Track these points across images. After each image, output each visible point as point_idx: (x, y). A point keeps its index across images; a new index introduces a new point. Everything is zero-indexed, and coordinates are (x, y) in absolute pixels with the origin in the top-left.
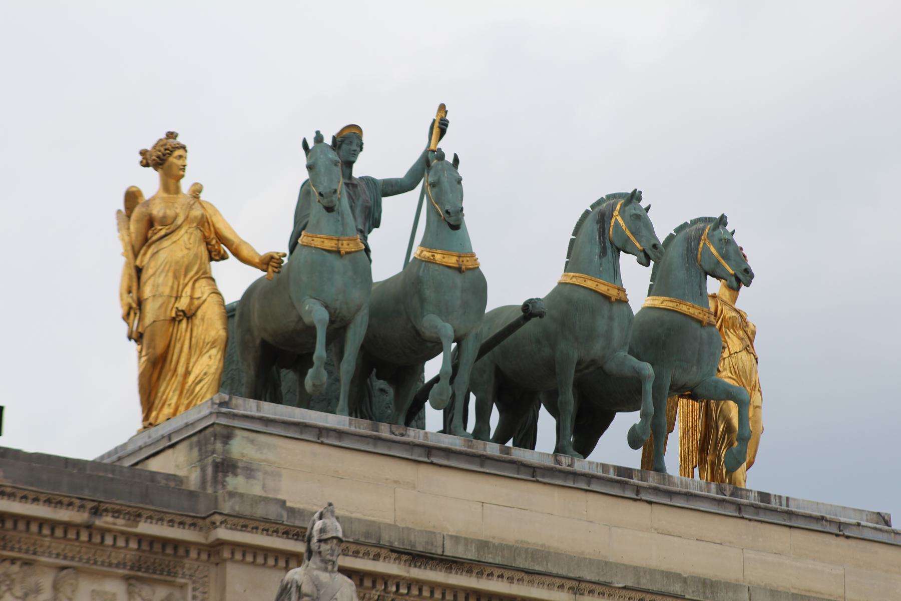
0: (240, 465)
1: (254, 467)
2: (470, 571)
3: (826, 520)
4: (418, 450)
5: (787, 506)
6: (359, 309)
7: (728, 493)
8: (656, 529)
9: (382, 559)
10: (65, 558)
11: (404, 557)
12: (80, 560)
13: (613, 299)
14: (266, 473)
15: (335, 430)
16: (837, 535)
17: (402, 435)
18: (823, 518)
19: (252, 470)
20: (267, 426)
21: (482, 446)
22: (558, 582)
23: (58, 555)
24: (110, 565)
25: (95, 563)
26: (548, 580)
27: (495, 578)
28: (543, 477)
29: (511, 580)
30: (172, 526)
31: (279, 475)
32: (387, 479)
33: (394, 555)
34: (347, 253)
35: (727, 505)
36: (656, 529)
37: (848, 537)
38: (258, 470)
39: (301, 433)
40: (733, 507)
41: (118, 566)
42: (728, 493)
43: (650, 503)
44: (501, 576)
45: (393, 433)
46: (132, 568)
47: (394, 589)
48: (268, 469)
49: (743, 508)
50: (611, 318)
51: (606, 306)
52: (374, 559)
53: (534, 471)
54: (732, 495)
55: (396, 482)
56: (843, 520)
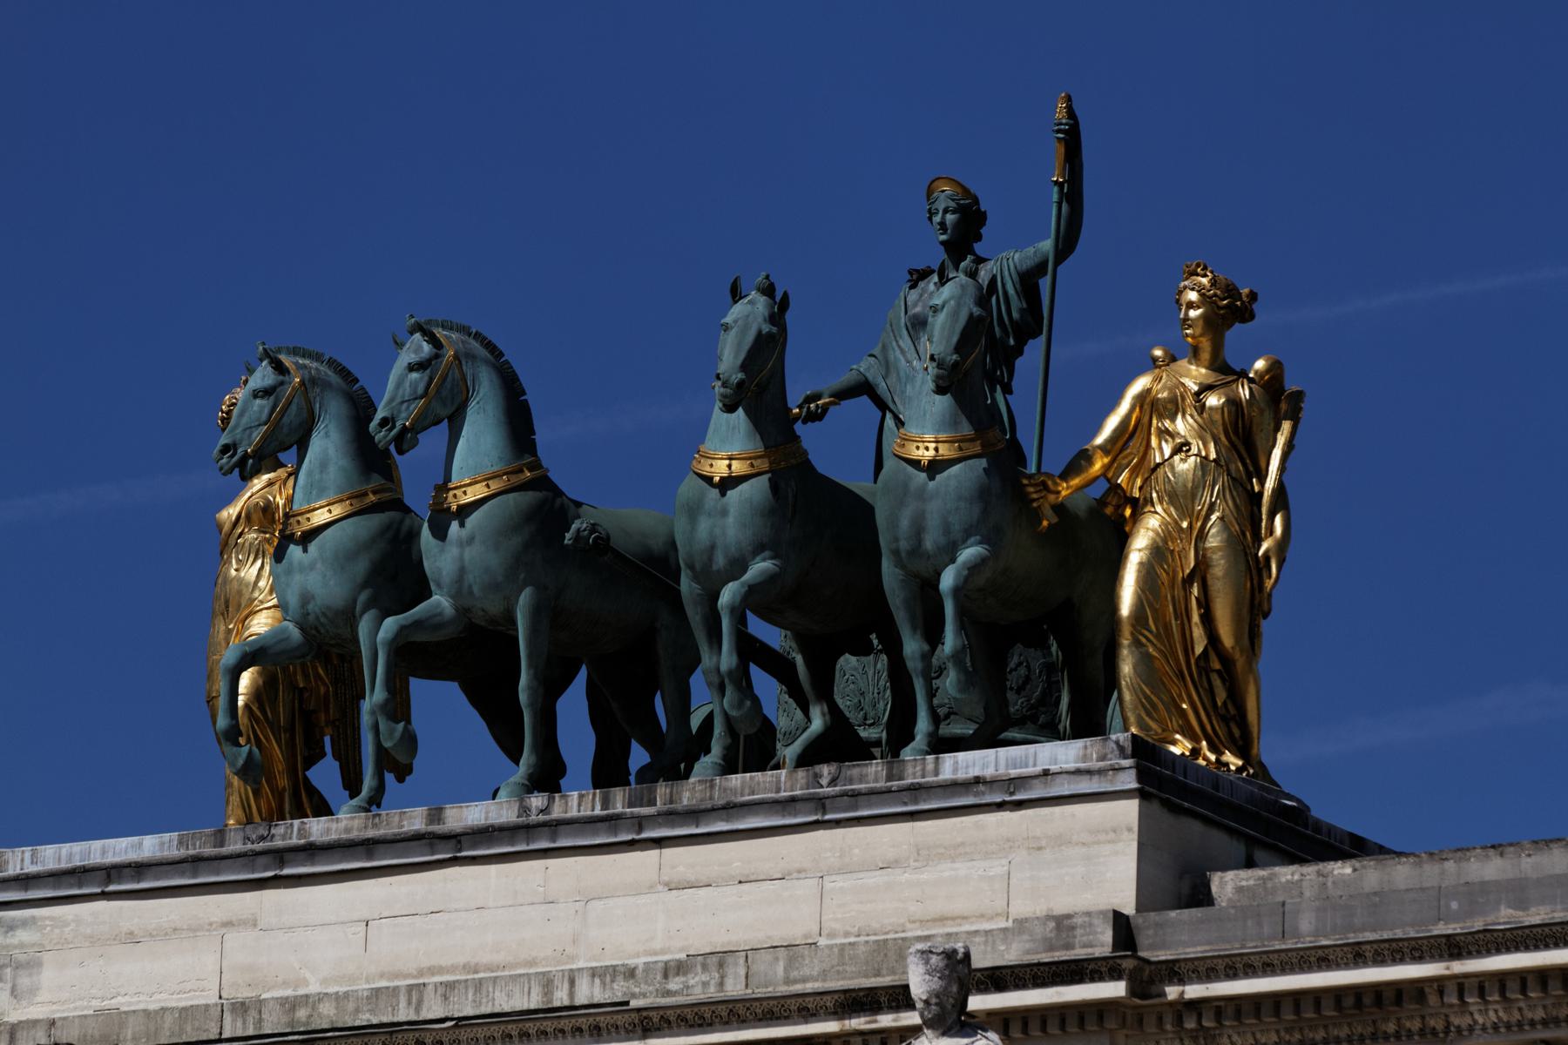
4: (262, 860)
5: (936, 773)
8: (666, 884)
14: (18, 966)
15: (129, 865)
16: (1000, 806)
17: (262, 838)
18: (978, 780)
20: (26, 890)
28: (474, 847)
31: (39, 964)
35: (799, 805)
36: (666, 884)
37: (1020, 805)
40: (811, 805)
42: (824, 782)
43: (659, 843)
45: (247, 839)
48: (22, 958)
49: (827, 802)
50: (724, 513)
51: (715, 492)
55: (228, 924)
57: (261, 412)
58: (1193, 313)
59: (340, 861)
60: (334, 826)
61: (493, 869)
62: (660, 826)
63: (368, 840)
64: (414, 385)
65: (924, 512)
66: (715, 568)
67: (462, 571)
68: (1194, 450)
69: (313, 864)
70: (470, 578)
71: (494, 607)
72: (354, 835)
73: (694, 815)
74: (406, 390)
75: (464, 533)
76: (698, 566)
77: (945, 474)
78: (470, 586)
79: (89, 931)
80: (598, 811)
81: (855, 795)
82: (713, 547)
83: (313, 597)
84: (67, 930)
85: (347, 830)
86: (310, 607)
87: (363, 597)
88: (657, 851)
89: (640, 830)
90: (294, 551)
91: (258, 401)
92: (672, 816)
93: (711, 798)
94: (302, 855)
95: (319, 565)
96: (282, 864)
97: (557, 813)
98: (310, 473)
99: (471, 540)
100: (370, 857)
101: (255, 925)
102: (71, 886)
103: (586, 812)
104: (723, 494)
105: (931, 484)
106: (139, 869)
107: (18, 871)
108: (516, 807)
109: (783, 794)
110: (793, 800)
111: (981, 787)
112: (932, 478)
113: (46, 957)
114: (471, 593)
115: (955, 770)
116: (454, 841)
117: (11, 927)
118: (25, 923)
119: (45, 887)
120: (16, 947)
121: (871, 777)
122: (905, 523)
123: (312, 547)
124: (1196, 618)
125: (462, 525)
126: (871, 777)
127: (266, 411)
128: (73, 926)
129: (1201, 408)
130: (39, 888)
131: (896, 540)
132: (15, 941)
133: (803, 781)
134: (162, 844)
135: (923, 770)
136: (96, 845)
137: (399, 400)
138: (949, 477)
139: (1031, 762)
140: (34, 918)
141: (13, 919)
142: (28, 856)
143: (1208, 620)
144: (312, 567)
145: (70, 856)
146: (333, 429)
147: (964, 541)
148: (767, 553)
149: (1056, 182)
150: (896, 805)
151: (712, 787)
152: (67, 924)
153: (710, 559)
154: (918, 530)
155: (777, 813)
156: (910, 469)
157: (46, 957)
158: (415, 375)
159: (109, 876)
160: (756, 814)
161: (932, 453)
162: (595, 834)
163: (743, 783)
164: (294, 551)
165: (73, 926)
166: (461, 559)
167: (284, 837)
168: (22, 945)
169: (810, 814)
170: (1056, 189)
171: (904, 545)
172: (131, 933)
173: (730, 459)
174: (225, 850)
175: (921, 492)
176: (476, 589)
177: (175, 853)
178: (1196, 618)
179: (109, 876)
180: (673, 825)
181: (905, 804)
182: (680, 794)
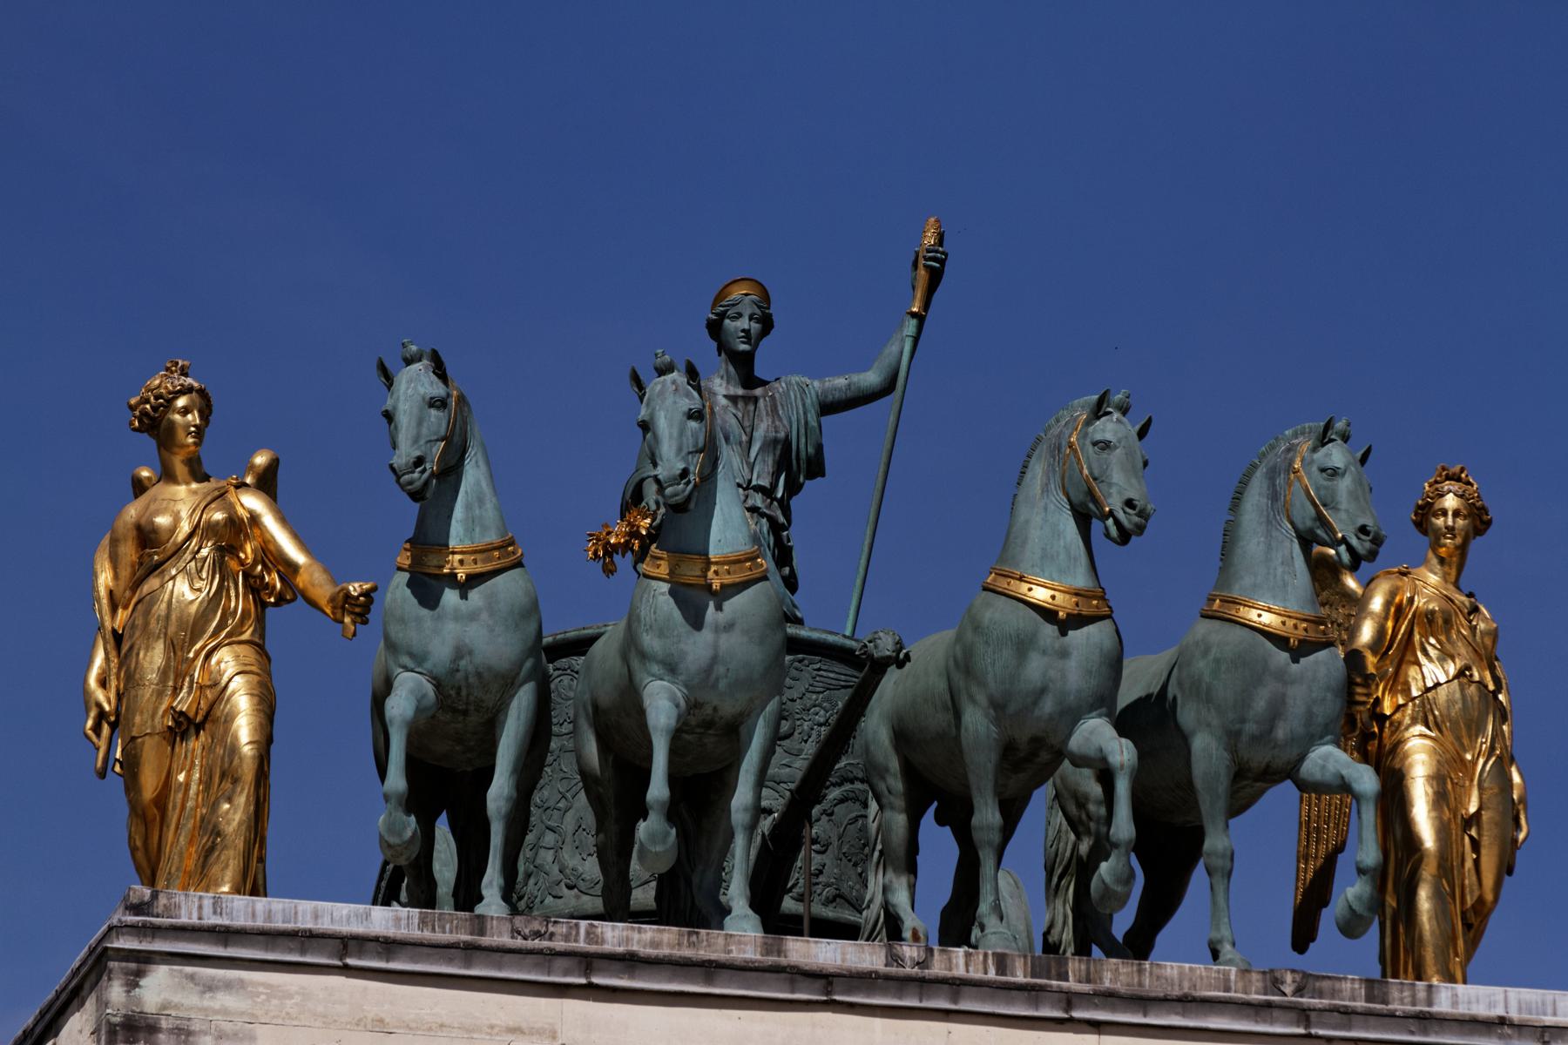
0: (164, 1024)
1: (195, 1027)
3: (1512, 1025)
4: (560, 963)
5: (1430, 1004)
6: (509, 684)
7: (1288, 989)
13: (1061, 614)
15: (376, 939)
17: (537, 935)
18: (1502, 1021)
19: (189, 1033)
20: (226, 946)
21: (721, 941)
28: (848, 992)
32: (492, 1027)
34: (475, 580)
35: (1276, 1013)
38: (205, 1033)
39: (303, 952)
40: (1293, 1015)
42: (1288, 989)
43: (1097, 1027)
45: (515, 932)
48: (227, 1027)
49: (1313, 1015)
50: (1064, 654)
51: (1050, 630)
53: (831, 983)
54: (1299, 991)
55: (515, 1030)
56: (1549, 1020)
57: (440, 425)
58: (1460, 522)
59: (670, 981)
60: (636, 936)
61: (878, 1023)
62: (1096, 1007)
63: (710, 962)
64: (695, 435)
65: (1284, 695)
66: (1037, 712)
67: (715, 660)
68: (1476, 677)
69: (632, 977)
70: (720, 669)
71: (728, 708)
72: (665, 951)
73: (1141, 1001)
74: (689, 444)
75: (722, 617)
76: (1012, 708)
77: (1312, 658)
78: (717, 679)
79: (320, 1009)
80: (992, 974)
81: (1347, 1012)
82: (1042, 691)
83: (471, 653)
84: (289, 1002)
85: (655, 944)
86: (463, 663)
87: (529, 664)
88: (1095, 1037)
89: (1069, 1006)
90: (450, 597)
91: (433, 412)
92: (1110, 998)
93: (1140, 984)
94: (617, 965)
95: (484, 616)
96: (588, 970)
97: (937, 969)
98: (468, 507)
99: (729, 627)
100: (709, 980)
101: (554, 1037)
102: (291, 951)
103: (976, 974)
104: (1064, 633)
105: (1294, 666)
106: (389, 946)
107: (195, 920)
108: (883, 954)
109: (1232, 994)
110: (1269, 1005)
111: (1507, 1030)
112: (1295, 660)
113: (260, 1030)
114: (714, 686)
115: (1455, 1003)
116: (820, 983)
117: (210, 987)
118: (228, 986)
119: (252, 946)
120: (217, 1012)
121: (1347, 994)
122: (1260, 704)
123: (474, 595)
124: (1469, 864)
125: (719, 608)
126: (1347, 994)
127: (444, 425)
128: (297, 999)
129: (1473, 629)
130: (244, 946)
131: (1243, 721)
132: (216, 1005)
133: (1260, 985)
134: (398, 920)
135: (1413, 996)
136: (1515, 994)
137: (685, 451)
138: (1316, 662)
139: (1550, 1010)
140: (241, 982)
141: (213, 979)
142: (208, 903)
143: (1477, 862)
144: (472, 617)
145: (269, 915)
146: (480, 455)
147: (1321, 737)
148: (1104, 710)
149: (913, 315)
150: (1400, 1032)
151: (1140, 971)
152: (290, 996)
153: (1035, 703)
154: (1276, 711)
155: (1247, 1017)
156: (1269, 645)
157: (260, 1030)
158: (693, 424)
159: (345, 947)
160: (1221, 1014)
161: (1301, 633)
162: (1010, 1002)
163: (1181, 974)
164: (450, 597)
165: (297, 999)
166: (716, 647)
167: (567, 938)
168: (225, 1011)
169: (1290, 1024)
170: (914, 322)
171: (1251, 728)
172: (381, 1021)
173: (1077, 594)
174: (486, 941)
175: (1281, 676)
176: (722, 685)
177: (415, 933)
178: (1469, 864)
179: (345, 947)
180: (1114, 1009)
181: (1412, 1033)
182: (1099, 973)
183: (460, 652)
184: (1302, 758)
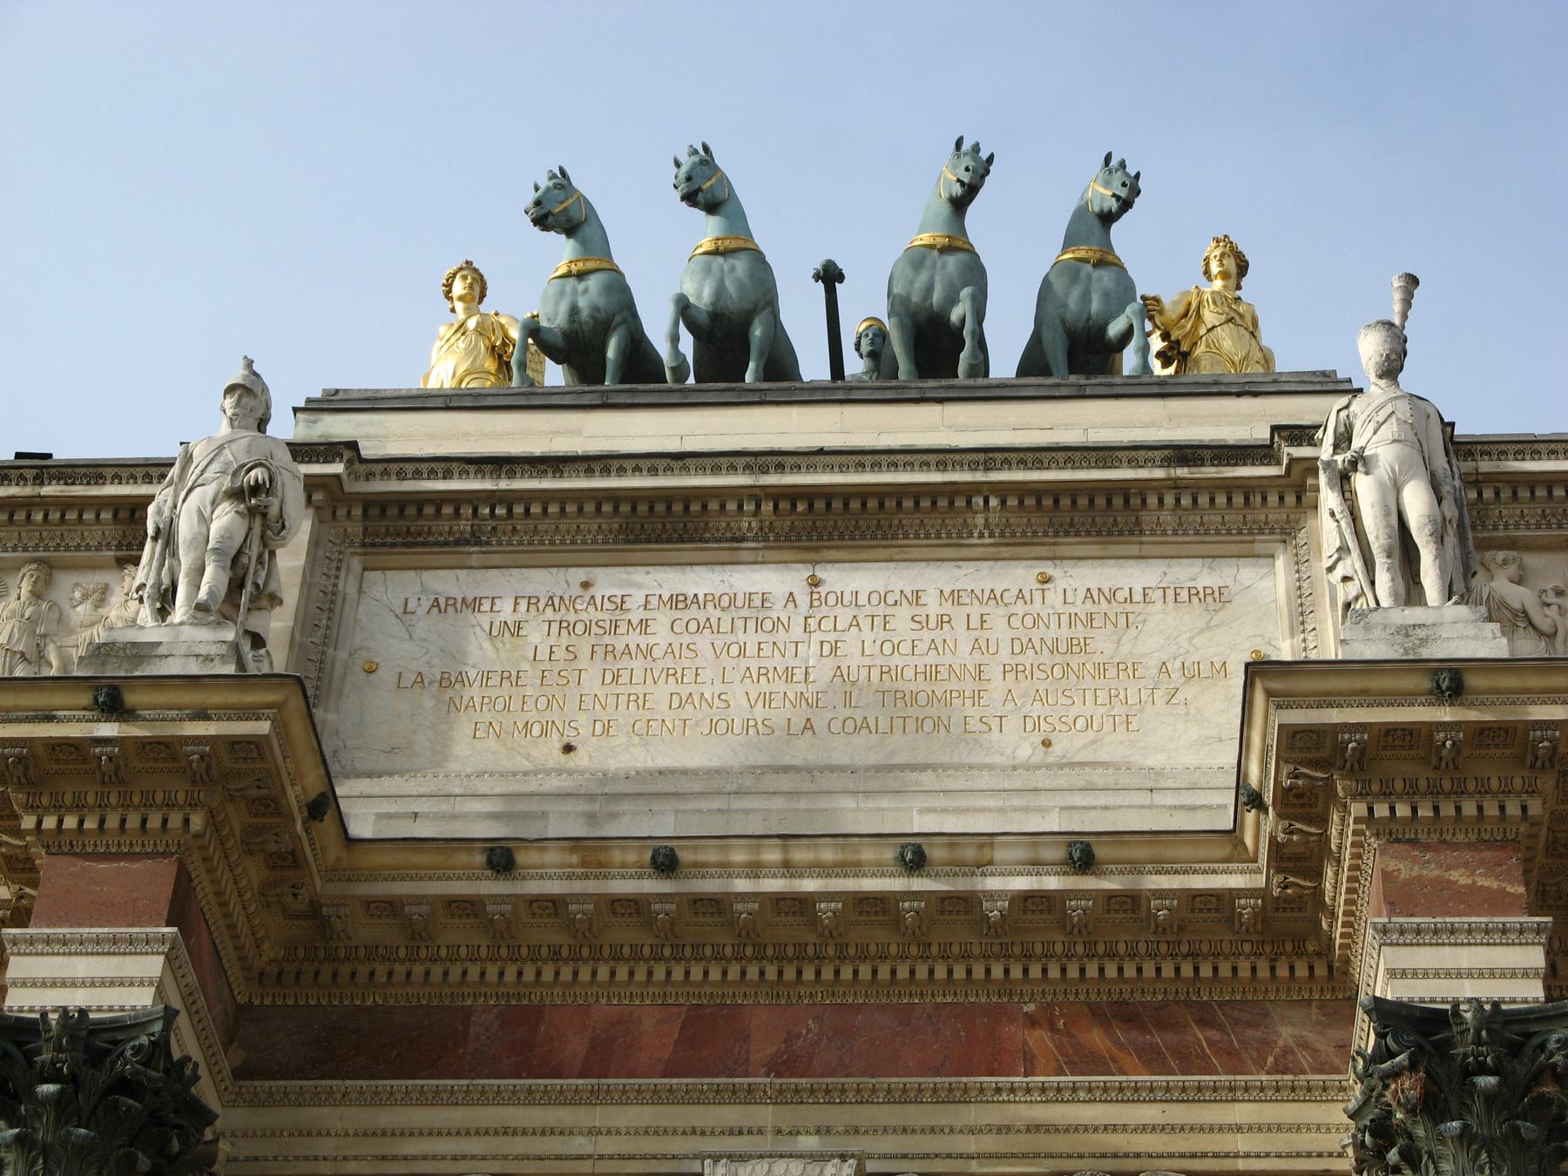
2: (590, 472)
9: (456, 475)
10: (25, 549)
11: (488, 468)
12: (47, 549)
22: (724, 461)
23: (15, 549)
24: (88, 548)
25: (67, 549)
26: (709, 462)
27: (629, 473)
29: (653, 472)
30: (151, 483)
33: (472, 468)
41: (99, 548)
44: (637, 469)
46: (119, 547)
47: (487, 511)
52: (444, 478)
183: (574, 311)
184: (1106, 324)
